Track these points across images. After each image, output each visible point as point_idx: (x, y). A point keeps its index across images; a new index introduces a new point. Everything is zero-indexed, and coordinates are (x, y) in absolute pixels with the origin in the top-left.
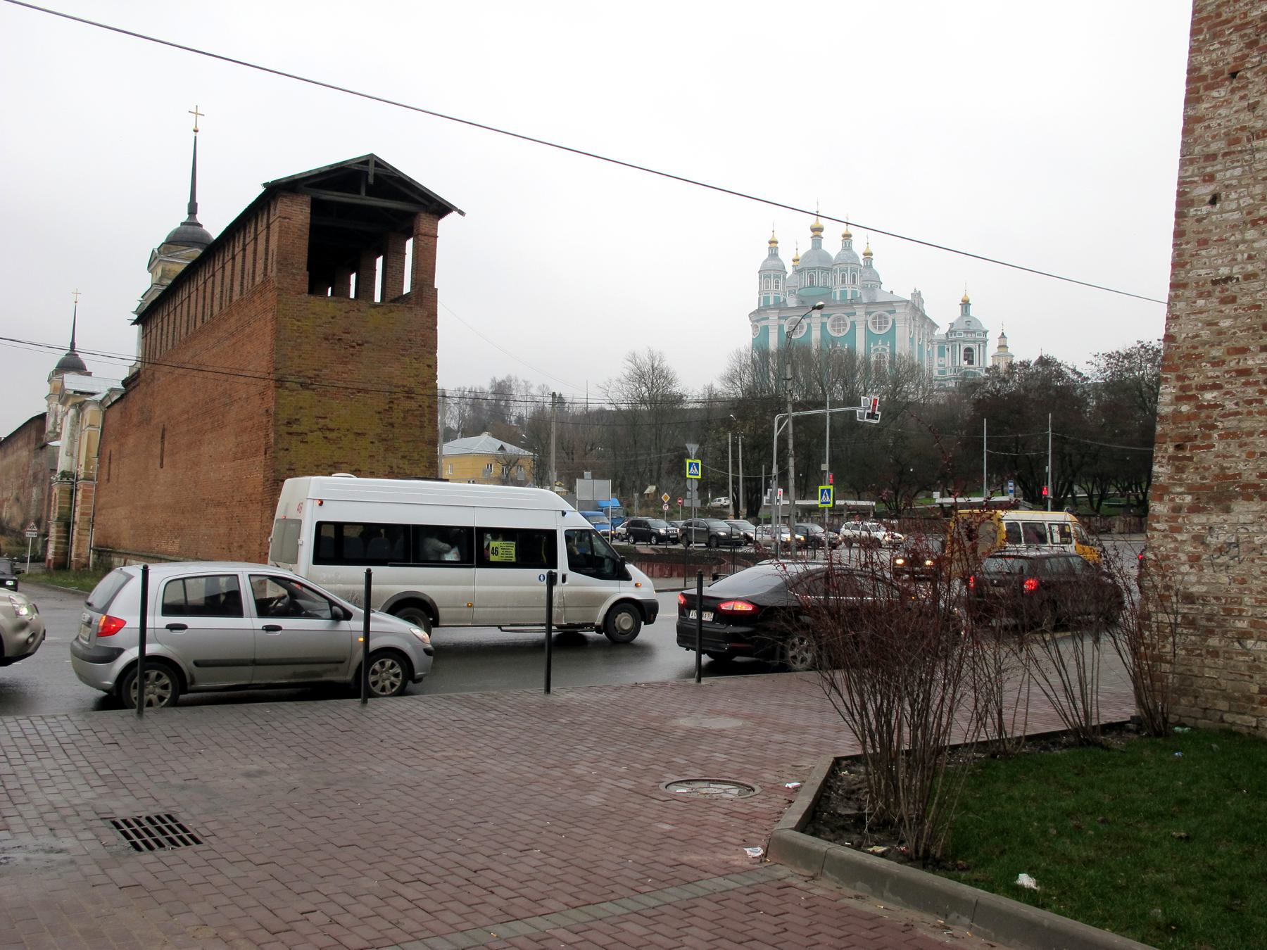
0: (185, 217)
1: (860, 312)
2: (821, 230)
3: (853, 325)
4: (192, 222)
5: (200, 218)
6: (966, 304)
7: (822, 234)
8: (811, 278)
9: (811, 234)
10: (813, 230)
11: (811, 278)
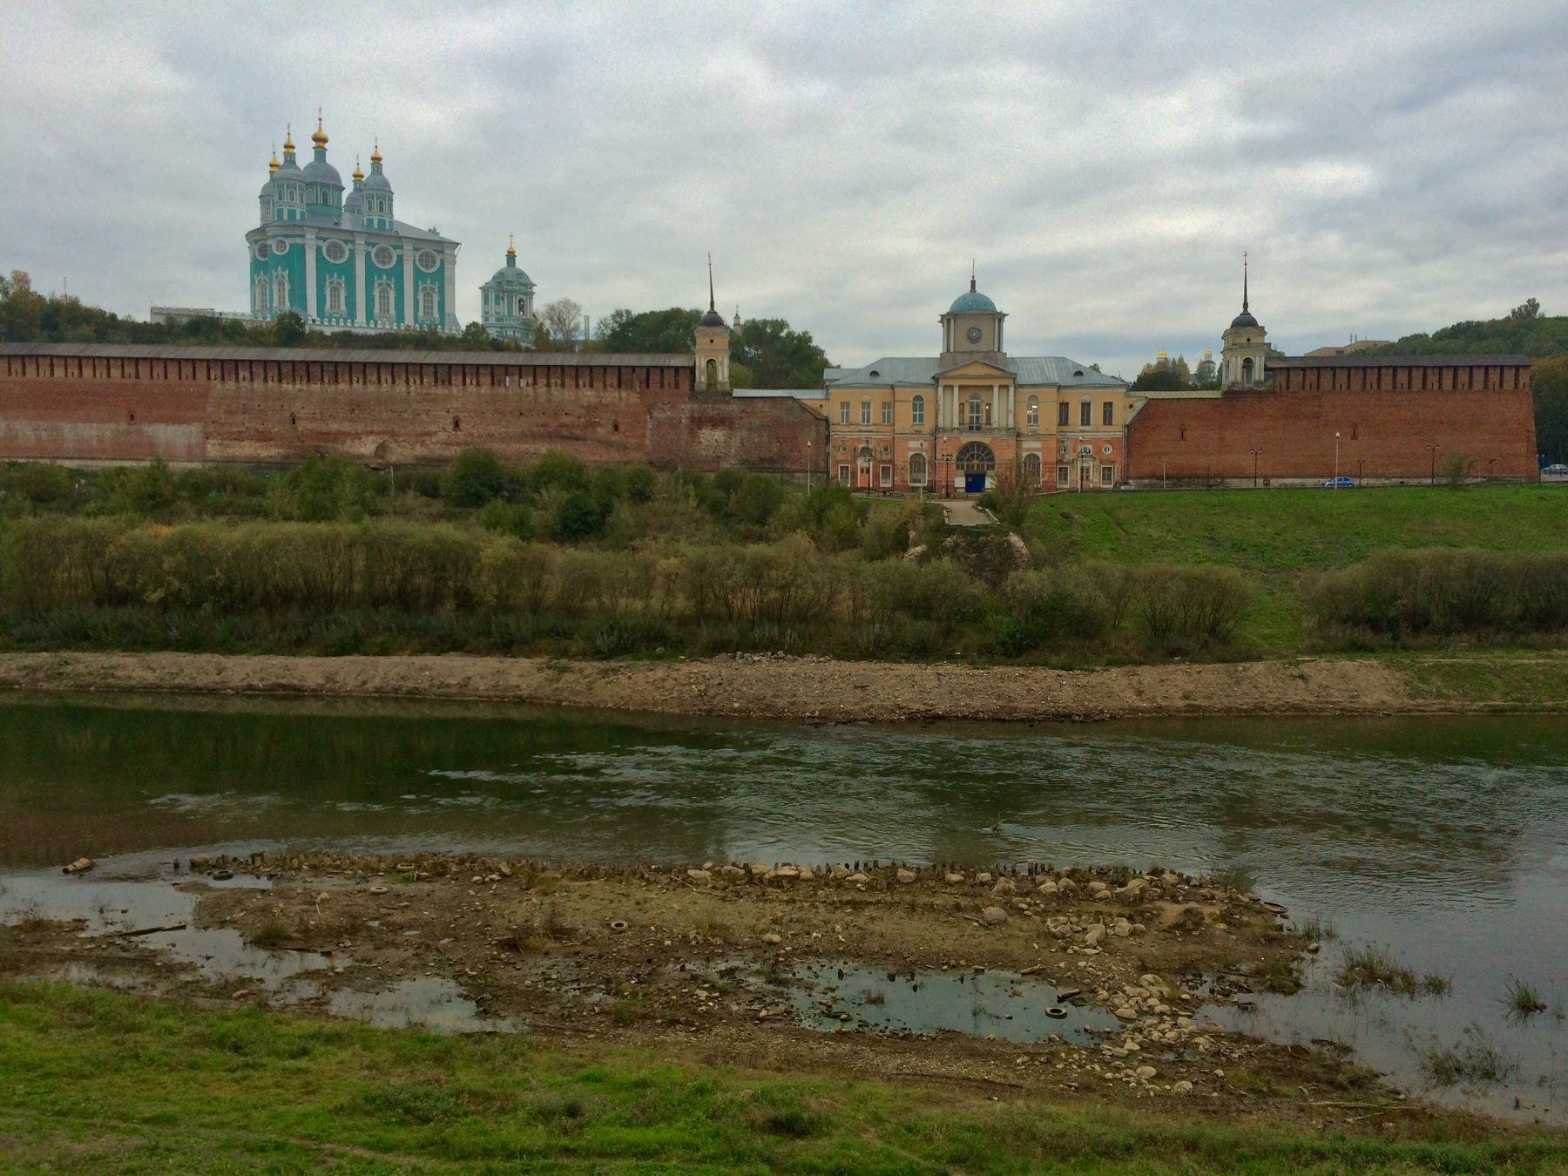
1: (408, 247)
2: (325, 141)
3: (400, 258)
4: (1246, 312)
5: (1249, 310)
6: (511, 257)
10: (316, 139)
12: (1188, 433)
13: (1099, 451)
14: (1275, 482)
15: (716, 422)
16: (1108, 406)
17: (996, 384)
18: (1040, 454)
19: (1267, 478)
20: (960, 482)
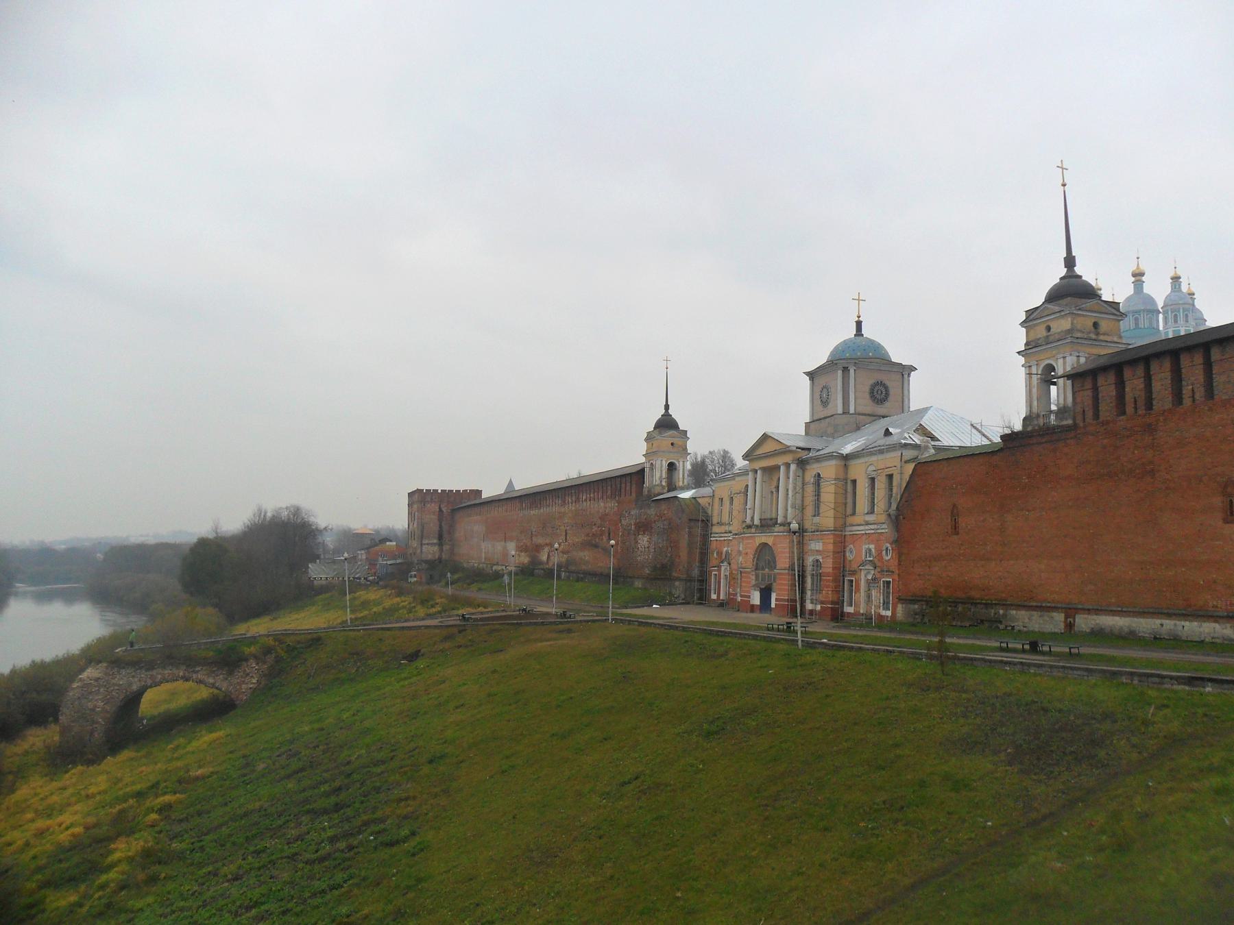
0: (1063, 271)
2: (1142, 274)
7: (1144, 278)
8: (1136, 319)
9: (1133, 279)
10: (1134, 275)
11: (1136, 319)
12: (962, 523)
13: (880, 554)
14: (1084, 622)
15: (644, 527)
16: (890, 477)
17: (779, 461)
18: (819, 558)
19: (1071, 612)
20: (756, 599)
